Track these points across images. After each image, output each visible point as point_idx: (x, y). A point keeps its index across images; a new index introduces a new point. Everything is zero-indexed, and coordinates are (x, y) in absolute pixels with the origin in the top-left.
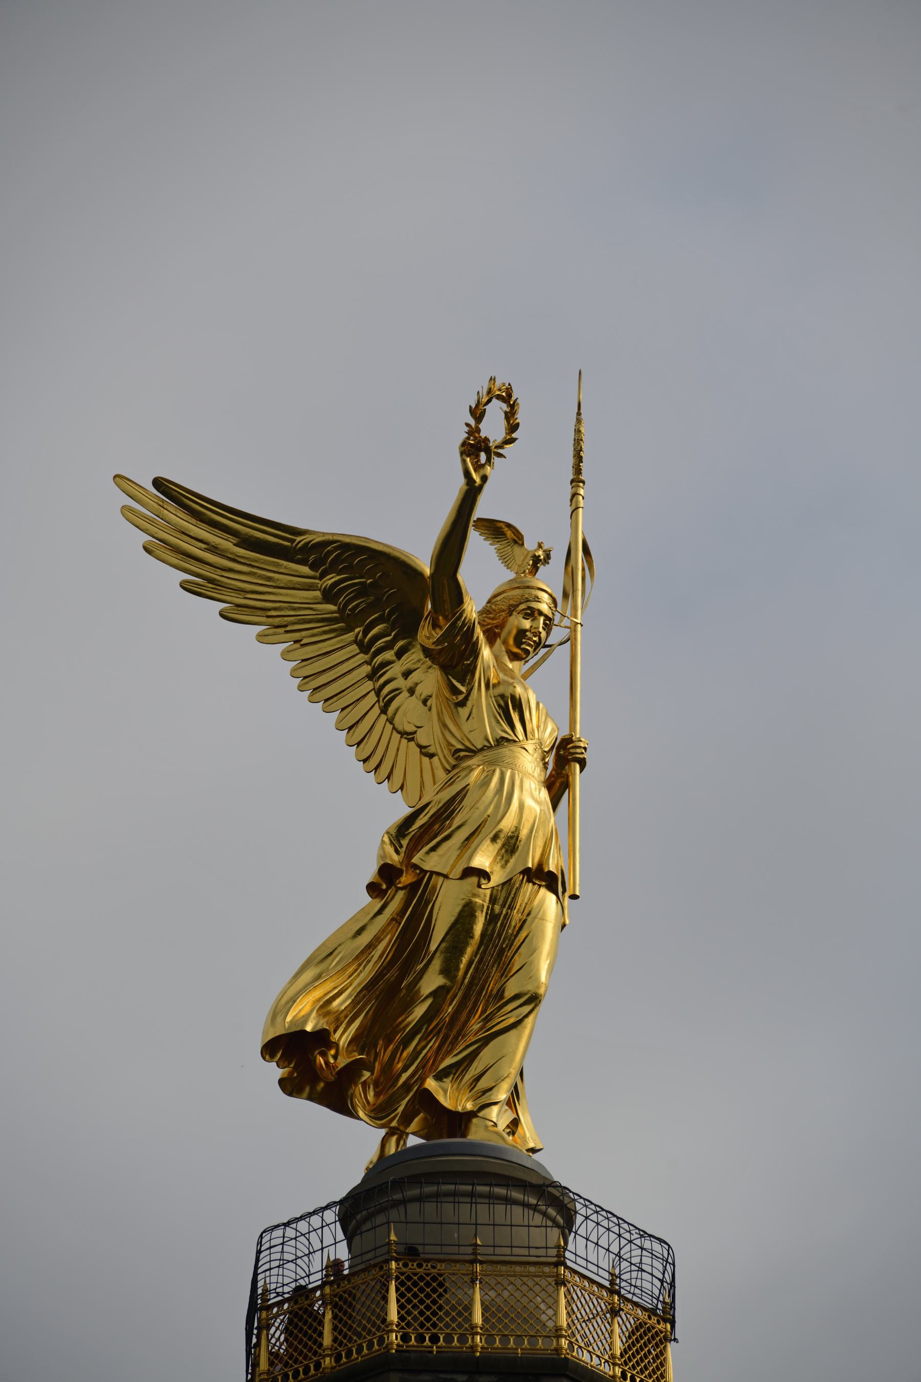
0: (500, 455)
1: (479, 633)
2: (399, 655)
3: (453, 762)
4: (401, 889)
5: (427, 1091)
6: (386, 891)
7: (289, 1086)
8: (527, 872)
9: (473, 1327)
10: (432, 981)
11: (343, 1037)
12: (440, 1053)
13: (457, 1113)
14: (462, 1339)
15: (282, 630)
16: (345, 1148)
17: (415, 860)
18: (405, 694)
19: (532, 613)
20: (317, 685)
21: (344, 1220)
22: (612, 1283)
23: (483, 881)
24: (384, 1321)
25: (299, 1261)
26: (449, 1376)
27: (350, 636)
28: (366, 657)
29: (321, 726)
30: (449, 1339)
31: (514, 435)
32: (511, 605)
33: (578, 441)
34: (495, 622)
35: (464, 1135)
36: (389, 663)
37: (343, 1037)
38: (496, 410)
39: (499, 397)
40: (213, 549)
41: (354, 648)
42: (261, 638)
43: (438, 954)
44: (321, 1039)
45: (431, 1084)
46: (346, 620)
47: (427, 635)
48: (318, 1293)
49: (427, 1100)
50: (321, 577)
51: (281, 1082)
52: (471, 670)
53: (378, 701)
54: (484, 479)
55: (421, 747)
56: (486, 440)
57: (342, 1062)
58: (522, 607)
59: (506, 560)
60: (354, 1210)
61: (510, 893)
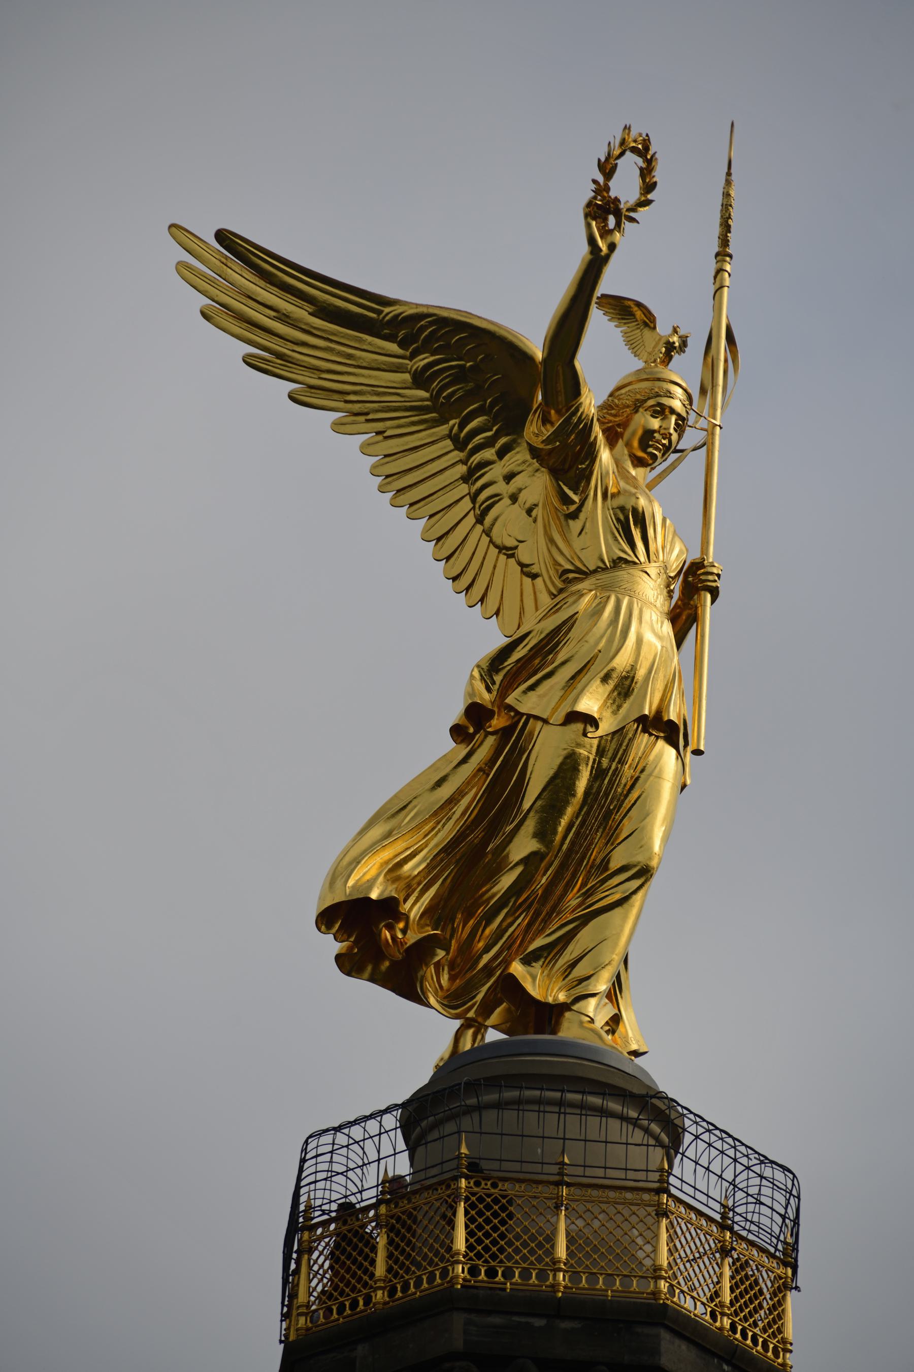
0: (632, 220)
1: (597, 431)
2: (501, 454)
3: (560, 585)
4: (492, 733)
5: (512, 977)
6: (472, 736)
7: (348, 964)
8: (642, 720)
9: (555, 1262)
10: (523, 845)
11: (414, 908)
12: (529, 932)
13: (547, 1005)
14: (542, 1275)
15: (362, 418)
16: (409, 1041)
17: (509, 700)
18: (506, 501)
19: (662, 411)
20: (400, 485)
21: (406, 1127)
22: (724, 1216)
23: (589, 729)
24: (449, 1249)
25: (350, 1174)
26: (523, 1319)
27: (443, 429)
28: (462, 455)
29: (404, 538)
30: (526, 1274)
31: (650, 197)
32: (637, 400)
33: (726, 207)
34: (617, 419)
35: (554, 1032)
36: (489, 463)
37: (414, 908)
38: (629, 165)
39: (634, 150)
40: (284, 318)
41: (448, 444)
42: (338, 427)
43: (532, 814)
44: (389, 909)
45: (517, 968)
46: (439, 410)
47: (535, 431)
48: (372, 1213)
49: (511, 988)
50: (412, 357)
51: (339, 959)
52: (587, 475)
53: (474, 508)
54: (612, 247)
55: (522, 565)
56: (617, 200)
57: (412, 937)
58: (651, 402)
59: (634, 346)
60: (421, 1116)
61: (621, 745)
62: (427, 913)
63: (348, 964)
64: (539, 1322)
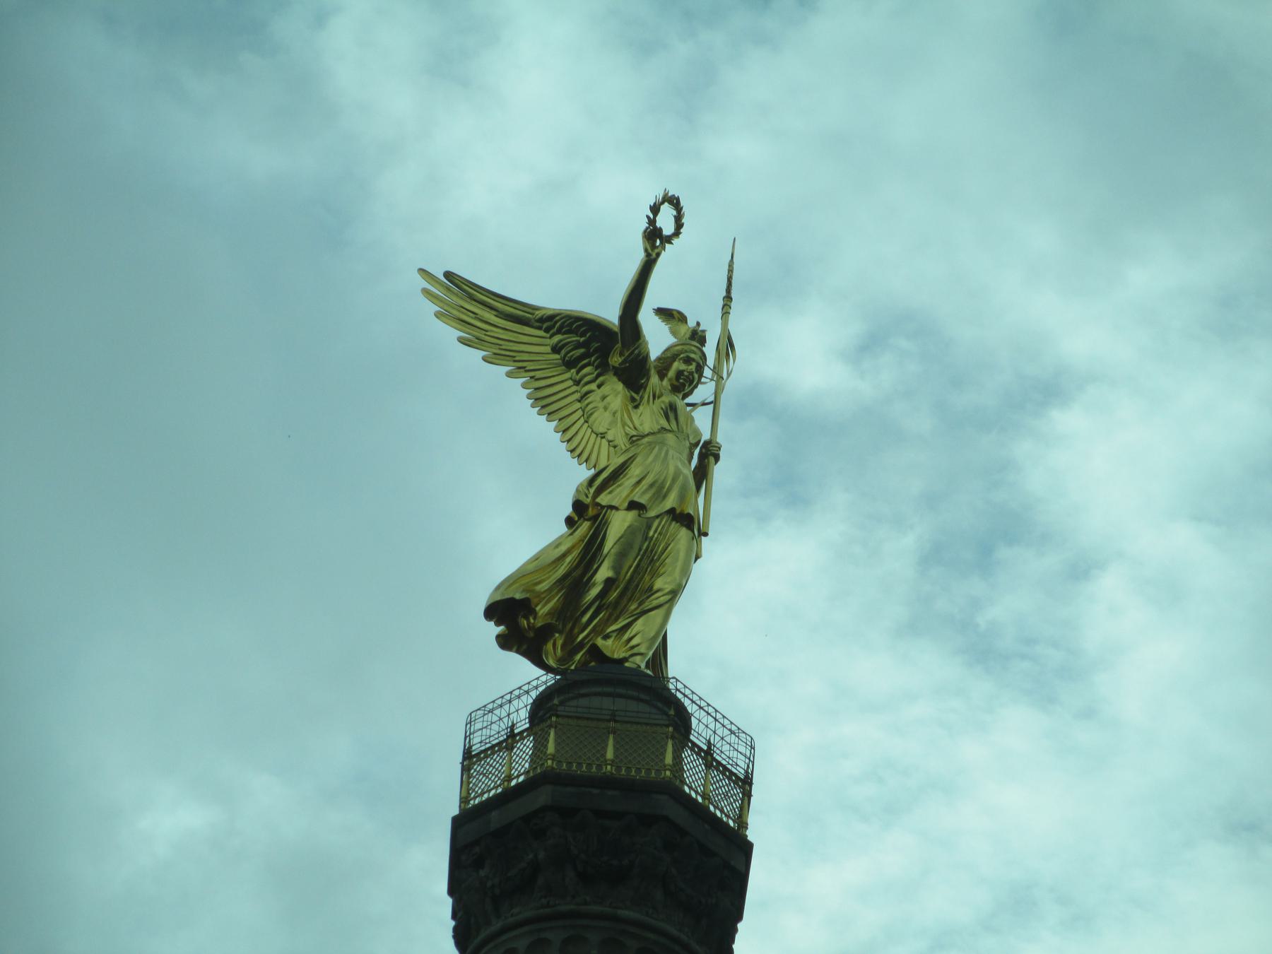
1: (653, 372)
2: (599, 387)
7: (505, 642)
10: (604, 573)
11: (543, 610)
14: (599, 767)
17: (598, 500)
18: (601, 410)
20: (544, 403)
22: (709, 747)
27: (568, 375)
29: (543, 430)
33: (731, 270)
37: (543, 610)
41: (570, 383)
45: (600, 642)
47: (615, 360)
49: (596, 652)
50: (551, 337)
52: (644, 387)
54: (658, 255)
55: (609, 442)
57: (539, 623)
59: (674, 333)
62: (549, 613)
63: (505, 642)
64: (595, 791)
